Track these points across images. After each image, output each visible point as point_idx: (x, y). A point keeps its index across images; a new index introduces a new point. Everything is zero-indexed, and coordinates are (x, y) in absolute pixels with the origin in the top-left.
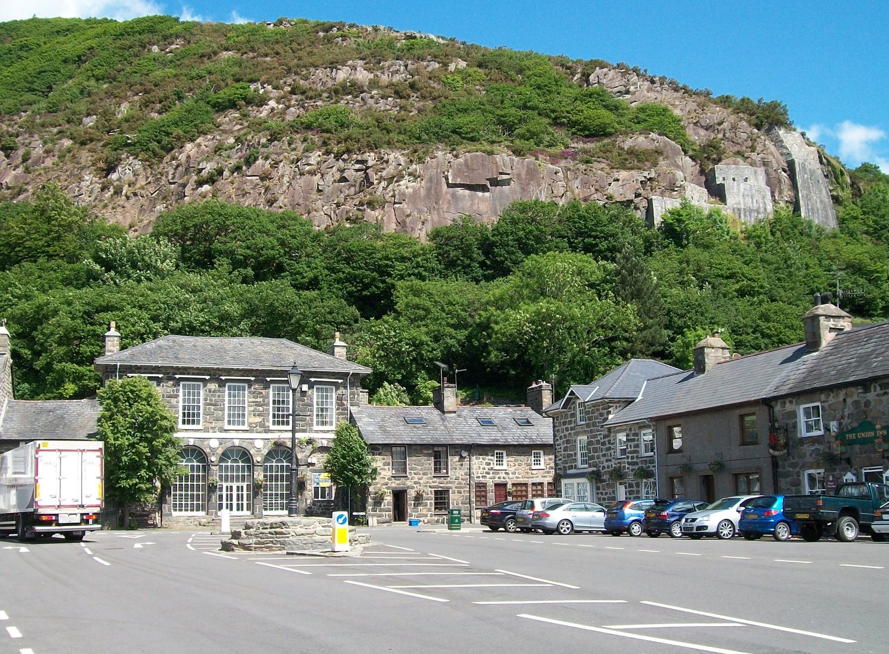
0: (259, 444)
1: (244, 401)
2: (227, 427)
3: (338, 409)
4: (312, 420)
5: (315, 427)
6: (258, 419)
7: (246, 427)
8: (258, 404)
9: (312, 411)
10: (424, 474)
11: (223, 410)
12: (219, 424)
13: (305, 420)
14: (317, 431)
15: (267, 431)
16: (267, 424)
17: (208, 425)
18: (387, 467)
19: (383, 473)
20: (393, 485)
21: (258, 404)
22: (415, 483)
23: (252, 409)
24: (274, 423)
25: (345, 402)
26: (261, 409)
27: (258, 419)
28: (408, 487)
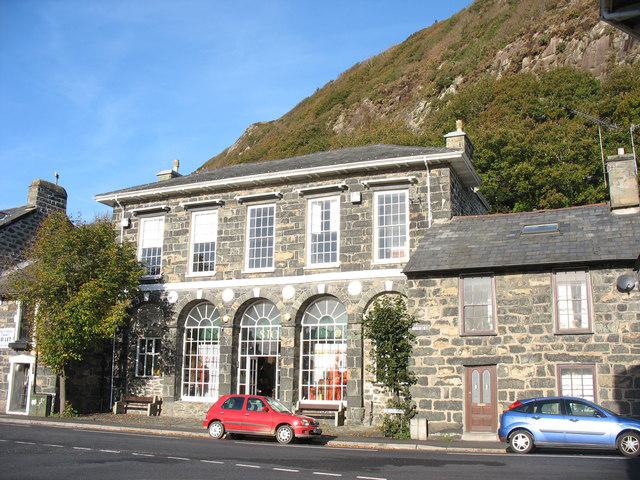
0: (288, 293)
1: (271, 230)
2: (247, 270)
3: (411, 227)
4: (369, 248)
5: (376, 260)
6: (287, 255)
7: (272, 269)
8: (288, 232)
9: (370, 233)
10: (533, 330)
11: (242, 244)
12: (236, 267)
13: (359, 249)
14: (377, 267)
15: (300, 272)
16: (301, 260)
17: (221, 268)
18: (450, 319)
19: (444, 330)
20: (465, 354)
21: (288, 232)
22: (513, 349)
23: (280, 240)
24: (314, 260)
25: (424, 214)
26: (293, 237)
27: (287, 255)
28: (498, 359)
